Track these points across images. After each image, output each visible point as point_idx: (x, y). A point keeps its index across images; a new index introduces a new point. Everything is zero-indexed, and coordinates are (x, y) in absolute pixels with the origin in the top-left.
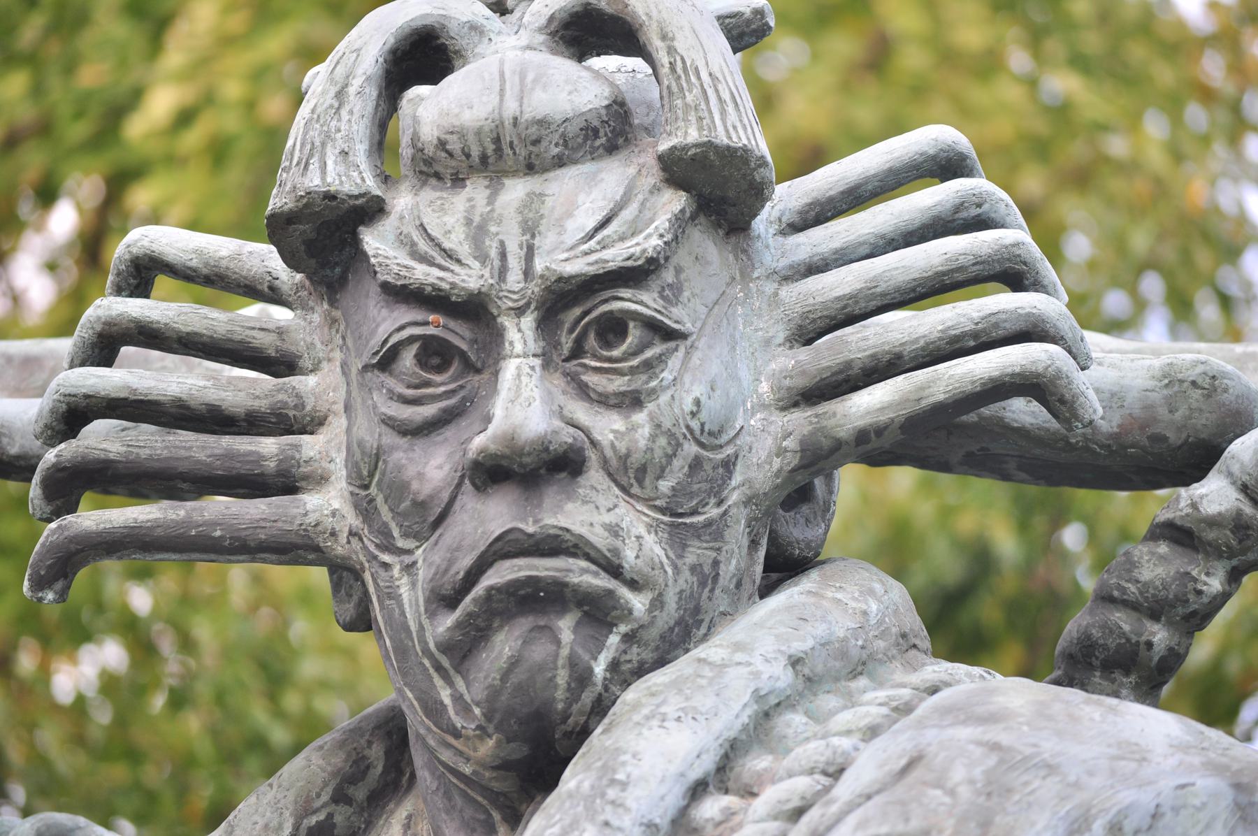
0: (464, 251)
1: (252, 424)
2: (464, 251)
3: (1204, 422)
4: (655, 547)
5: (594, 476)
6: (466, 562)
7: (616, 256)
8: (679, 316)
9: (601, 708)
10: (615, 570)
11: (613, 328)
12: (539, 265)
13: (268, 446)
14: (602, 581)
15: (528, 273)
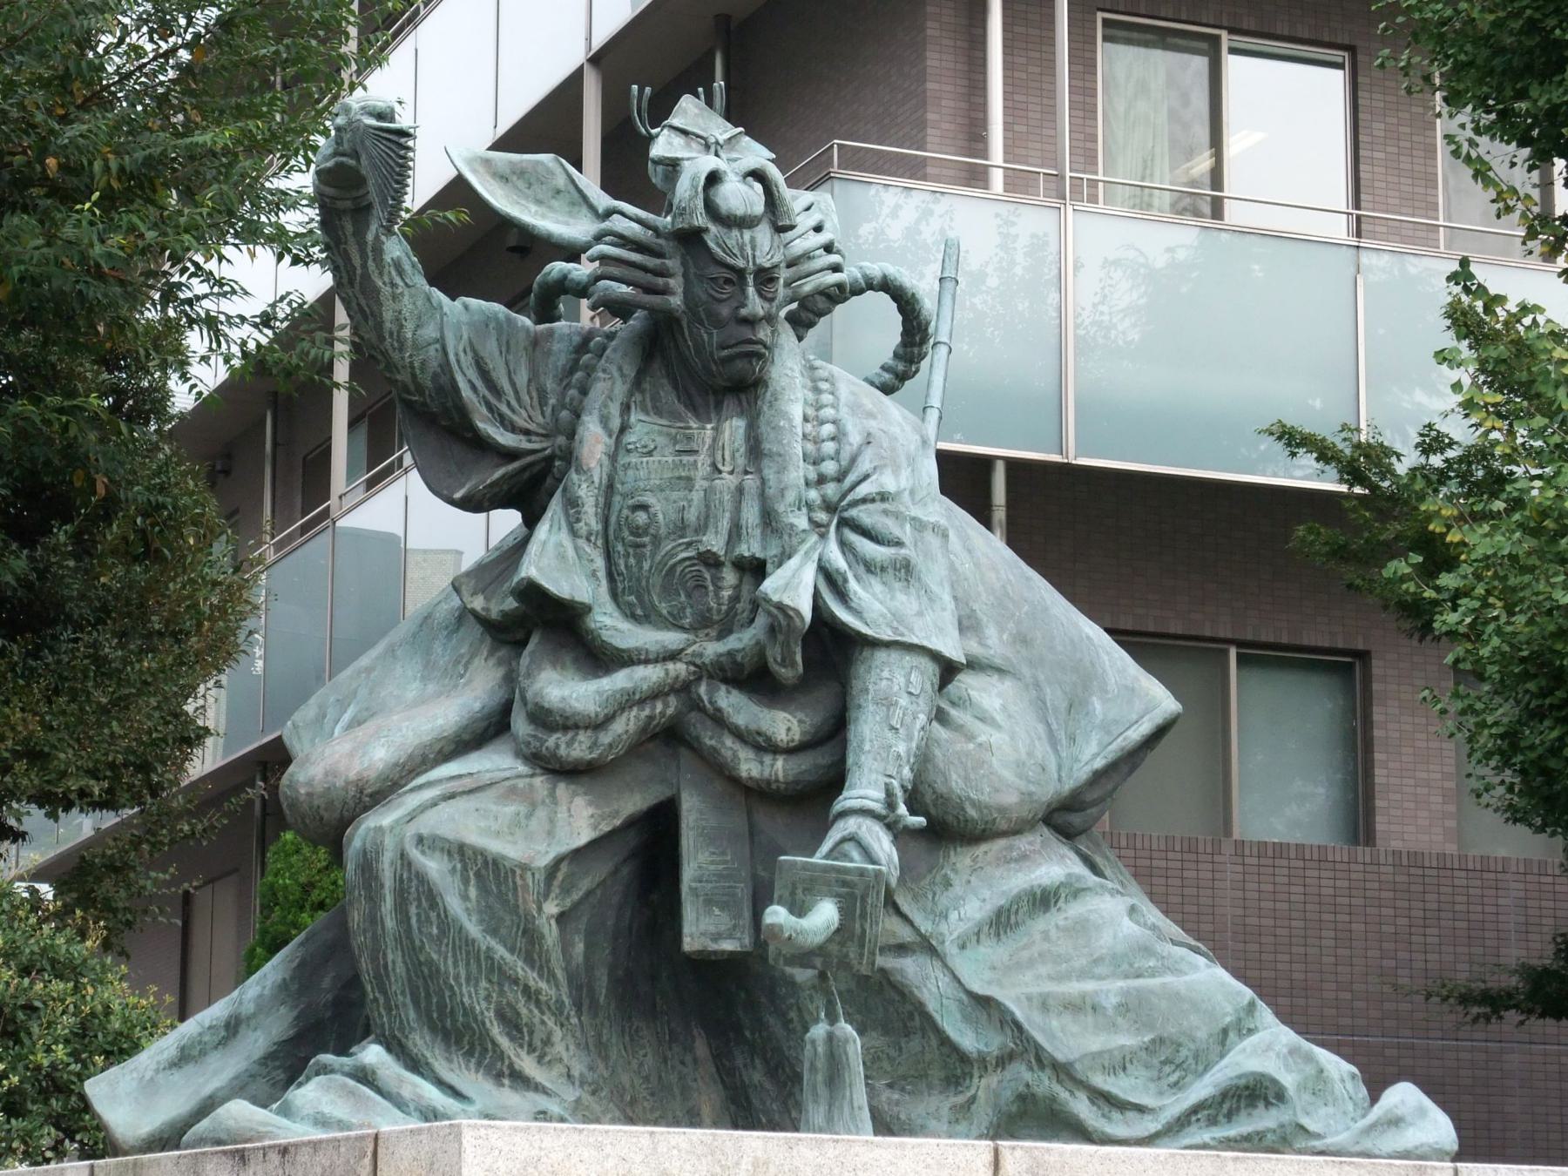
0: (738, 254)
2: (738, 254)
6: (733, 342)
12: (758, 261)
13: (660, 281)
15: (754, 263)
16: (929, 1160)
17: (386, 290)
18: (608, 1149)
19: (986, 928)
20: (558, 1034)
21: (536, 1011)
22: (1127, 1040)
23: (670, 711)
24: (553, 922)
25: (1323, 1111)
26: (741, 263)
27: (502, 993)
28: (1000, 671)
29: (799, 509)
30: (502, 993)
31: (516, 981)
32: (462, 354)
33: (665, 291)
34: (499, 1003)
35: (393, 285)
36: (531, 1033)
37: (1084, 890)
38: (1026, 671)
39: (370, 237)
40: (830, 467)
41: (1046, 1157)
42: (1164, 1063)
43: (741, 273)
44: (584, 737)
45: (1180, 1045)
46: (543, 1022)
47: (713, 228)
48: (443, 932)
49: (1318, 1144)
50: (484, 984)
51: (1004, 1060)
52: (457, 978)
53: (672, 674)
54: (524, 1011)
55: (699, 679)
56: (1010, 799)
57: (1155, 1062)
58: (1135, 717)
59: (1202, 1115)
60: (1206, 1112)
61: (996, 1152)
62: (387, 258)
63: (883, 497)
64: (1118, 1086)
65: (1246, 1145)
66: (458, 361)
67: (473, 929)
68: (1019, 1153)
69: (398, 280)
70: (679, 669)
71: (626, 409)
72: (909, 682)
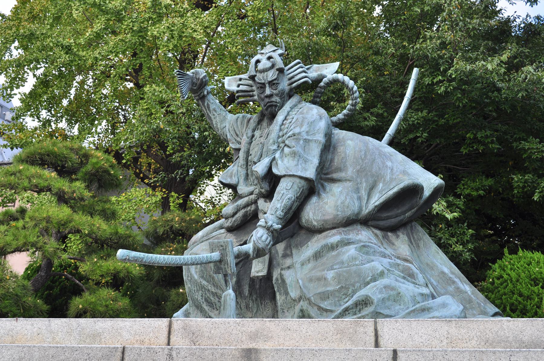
1: (250, 91)
3: (321, 78)
4: (279, 100)
7: (273, 78)
8: (279, 82)
9: (277, 113)
10: (276, 102)
11: (274, 84)
13: (251, 93)
16: (145, 325)
17: (212, 117)
18: (35, 325)
19: (312, 258)
23: (252, 209)
25: (397, 307)
26: (263, 81)
27: (205, 294)
30: (205, 294)
31: (209, 290)
33: (253, 96)
34: (205, 297)
35: (214, 115)
36: (216, 305)
39: (206, 104)
40: (285, 131)
41: (190, 323)
43: (264, 84)
44: (230, 220)
48: (191, 279)
51: (300, 298)
52: (194, 291)
53: (250, 198)
54: (212, 299)
55: (258, 198)
62: (211, 109)
63: (294, 135)
64: (325, 305)
67: (196, 277)
68: (179, 322)
69: (215, 113)
70: (253, 197)
71: (254, 130)
72: (287, 186)
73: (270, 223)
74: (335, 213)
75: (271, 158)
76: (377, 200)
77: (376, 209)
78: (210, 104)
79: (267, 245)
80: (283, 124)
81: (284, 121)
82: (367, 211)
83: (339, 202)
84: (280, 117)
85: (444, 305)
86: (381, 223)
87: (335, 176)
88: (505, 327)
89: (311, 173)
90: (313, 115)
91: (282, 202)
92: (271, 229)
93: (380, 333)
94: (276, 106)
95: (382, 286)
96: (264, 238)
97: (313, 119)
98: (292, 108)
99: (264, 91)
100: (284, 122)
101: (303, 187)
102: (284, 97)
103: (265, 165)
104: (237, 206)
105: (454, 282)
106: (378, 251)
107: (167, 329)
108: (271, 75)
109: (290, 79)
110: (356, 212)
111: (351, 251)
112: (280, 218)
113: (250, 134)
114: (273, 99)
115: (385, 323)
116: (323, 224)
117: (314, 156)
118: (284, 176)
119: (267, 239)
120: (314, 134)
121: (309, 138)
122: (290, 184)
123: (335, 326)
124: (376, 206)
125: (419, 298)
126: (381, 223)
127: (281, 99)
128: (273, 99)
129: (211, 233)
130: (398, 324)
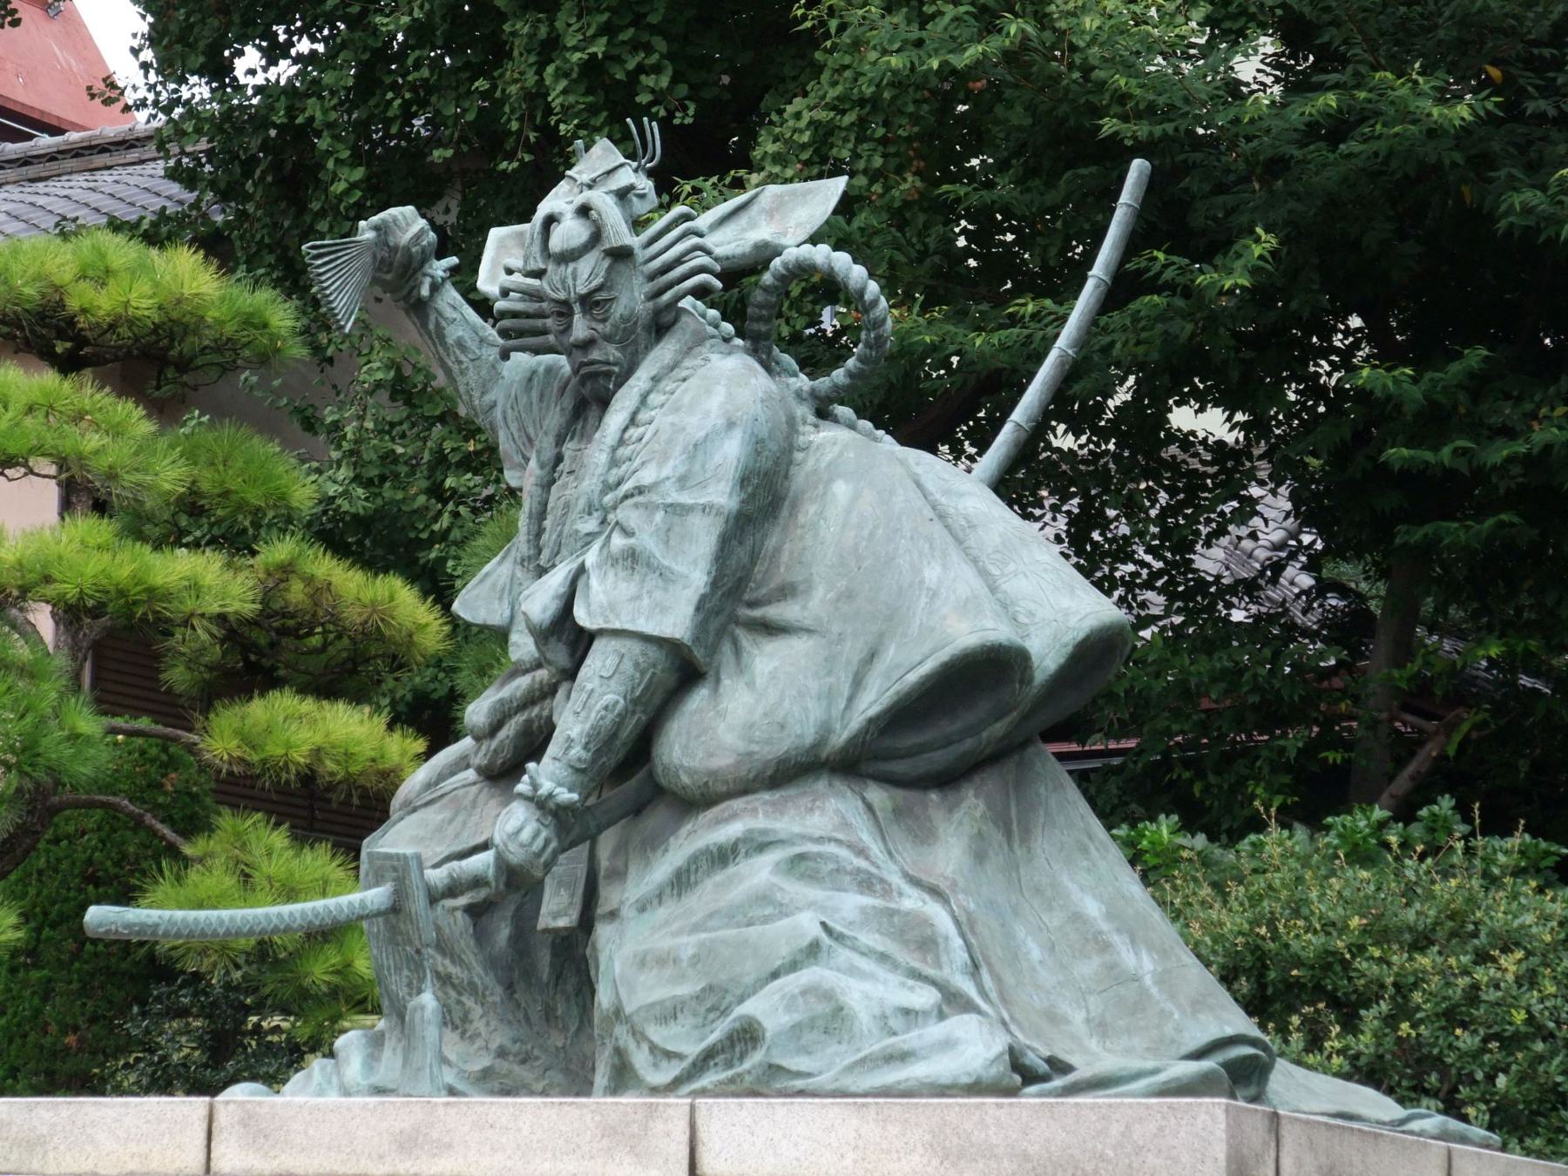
4: (618, 354)
5: (600, 341)
7: (595, 283)
8: (614, 293)
9: (614, 393)
11: (597, 303)
13: (539, 323)
14: (605, 368)
16: (150, 1117)
17: (455, 368)
19: (668, 891)
20: (477, 1011)
21: (453, 994)
22: (685, 990)
24: (459, 914)
26: (562, 296)
28: (809, 631)
29: (590, 514)
32: (509, 411)
33: (544, 332)
35: (460, 362)
37: (771, 843)
38: (836, 628)
39: (431, 326)
42: (710, 1010)
43: (566, 303)
45: (727, 991)
46: (459, 1002)
47: (551, 267)
49: (799, 1084)
50: (406, 972)
53: (538, 679)
56: (723, 761)
57: (702, 1010)
58: (918, 658)
59: (720, 1059)
60: (722, 1056)
61: (693, 1108)
62: (450, 341)
63: (640, 490)
65: (732, 1088)
66: (505, 418)
68: (232, 1107)
69: (463, 358)
71: (560, 440)
73: (543, 791)
74: (742, 746)
75: (574, 566)
76: (873, 700)
77: (872, 728)
78: (444, 324)
79: (538, 855)
80: (621, 442)
81: (625, 430)
82: (845, 735)
83: (760, 711)
84: (615, 419)
85: (948, 1044)
86: (899, 767)
87: (773, 612)
88: (989, 1120)
89: (676, 622)
90: (707, 414)
91: (587, 718)
92: (551, 805)
93: (703, 1134)
94: (608, 375)
95: (797, 991)
96: (525, 835)
97: (702, 433)
98: (656, 380)
99: (568, 328)
100: (627, 436)
101: (654, 666)
102: (635, 342)
103: (551, 592)
104: (501, 702)
105: (1105, 947)
106: (849, 868)
107: (205, 1126)
108: (587, 273)
109: (652, 277)
110: (809, 739)
111: (759, 871)
112: (577, 770)
113: (549, 453)
114: (595, 355)
115: (715, 1109)
116: (706, 784)
117: (695, 563)
118: (601, 632)
119: (536, 835)
120: (703, 485)
121: (686, 498)
122: (611, 661)
123: (597, 1118)
124: (871, 721)
125: (895, 1023)
126: (899, 767)
127: (623, 349)
128: (595, 355)
129: (453, 774)
130: (744, 1113)
